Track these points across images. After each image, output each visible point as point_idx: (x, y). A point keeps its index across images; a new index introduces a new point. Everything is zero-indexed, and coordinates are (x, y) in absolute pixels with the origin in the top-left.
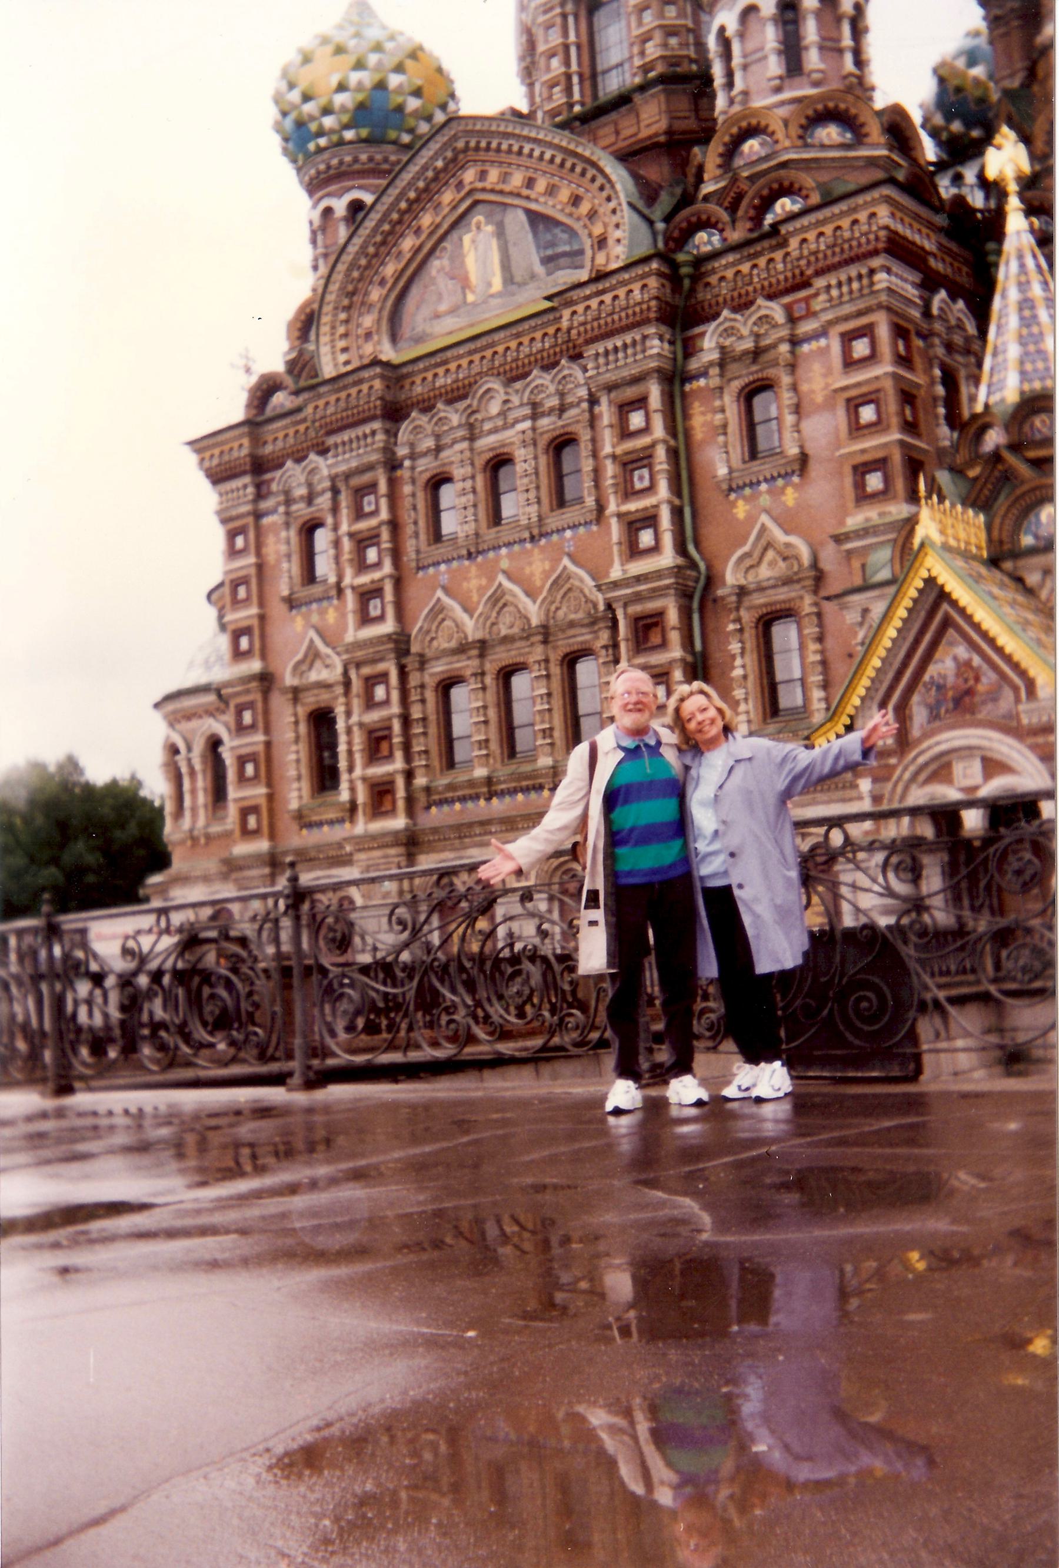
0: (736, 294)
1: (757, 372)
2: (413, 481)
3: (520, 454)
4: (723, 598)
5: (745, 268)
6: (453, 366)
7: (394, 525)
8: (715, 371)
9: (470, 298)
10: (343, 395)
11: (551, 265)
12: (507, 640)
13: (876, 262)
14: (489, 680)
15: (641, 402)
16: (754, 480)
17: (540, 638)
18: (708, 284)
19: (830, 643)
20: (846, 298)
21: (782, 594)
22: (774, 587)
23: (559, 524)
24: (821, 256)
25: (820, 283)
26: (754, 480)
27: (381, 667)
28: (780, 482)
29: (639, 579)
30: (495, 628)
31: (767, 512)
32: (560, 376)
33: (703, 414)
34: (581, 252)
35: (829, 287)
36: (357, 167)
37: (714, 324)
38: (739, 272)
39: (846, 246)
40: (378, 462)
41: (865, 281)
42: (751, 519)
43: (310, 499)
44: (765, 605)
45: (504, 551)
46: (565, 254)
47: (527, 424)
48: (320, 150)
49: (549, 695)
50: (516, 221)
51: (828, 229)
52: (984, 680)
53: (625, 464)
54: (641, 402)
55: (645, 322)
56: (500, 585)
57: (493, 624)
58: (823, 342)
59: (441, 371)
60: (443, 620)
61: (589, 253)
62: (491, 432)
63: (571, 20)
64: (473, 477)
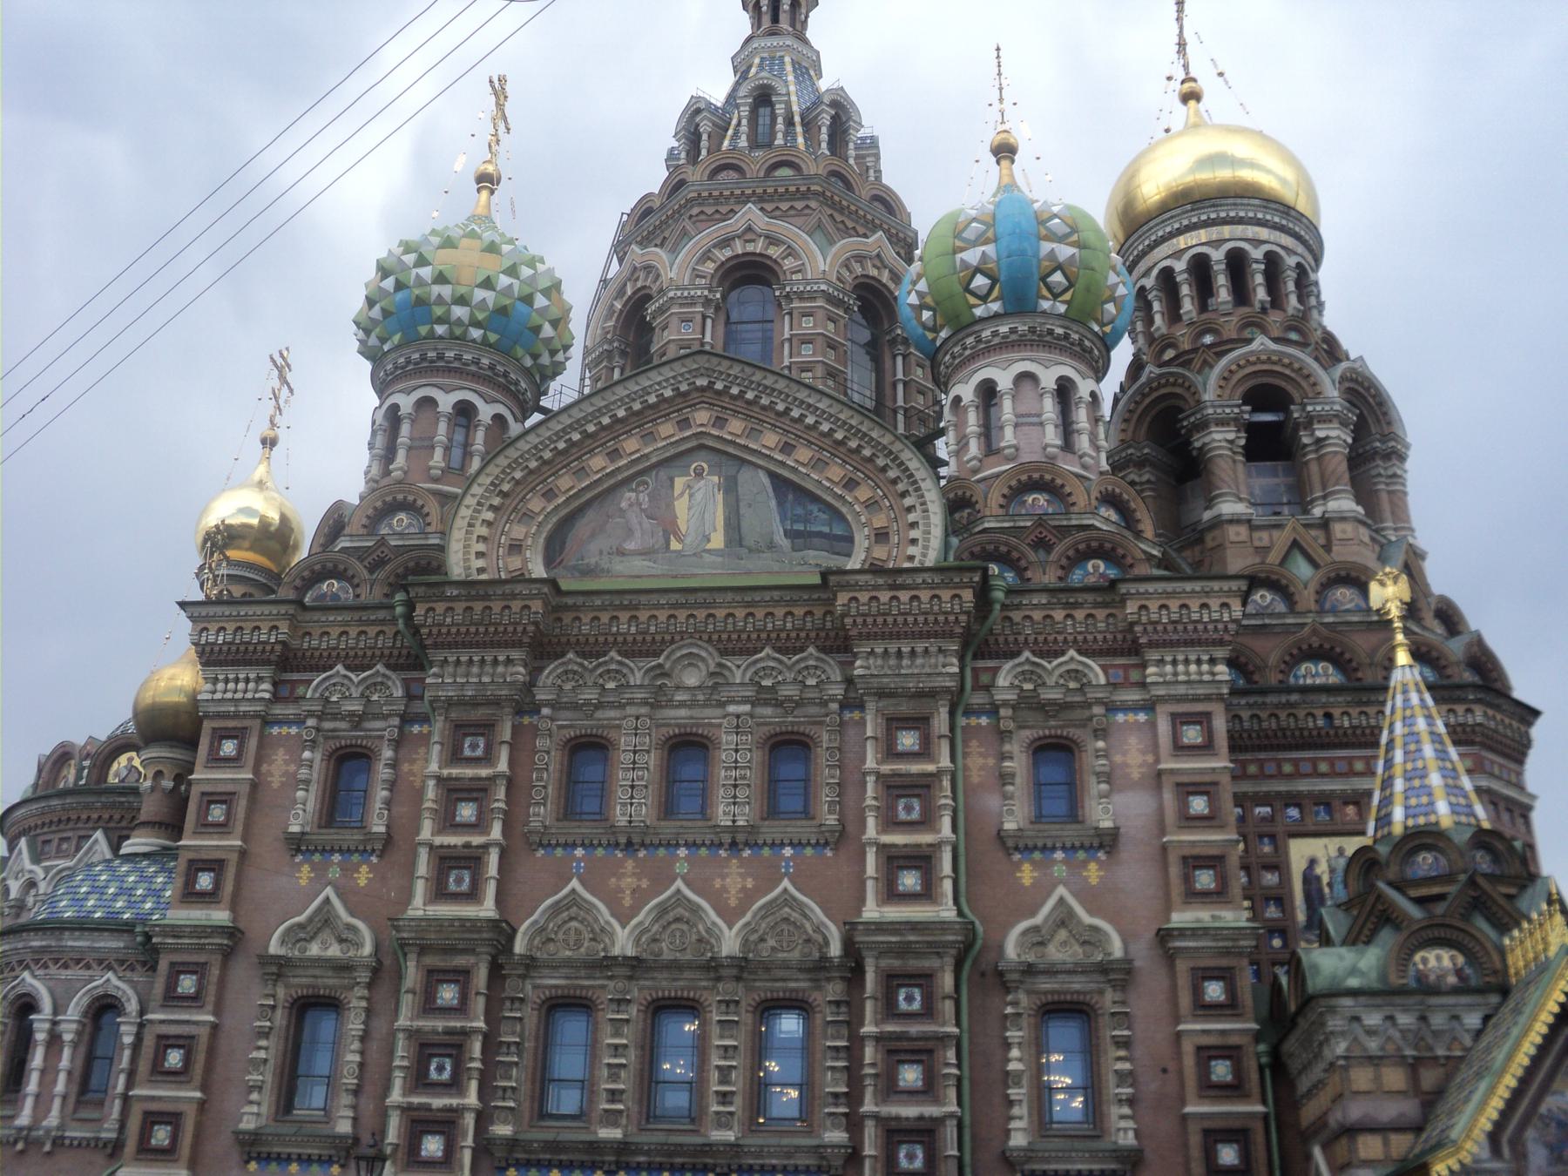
0: (1041, 638)
1: (1056, 727)
2: (550, 736)
3: (727, 739)
4: (1001, 974)
5: (1059, 615)
6: (643, 616)
7: (511, 783)
9: (675, 545)
10: (478, 606)
11: (801, 541)
12: (675, 966)
13: (1220, 653)
14: (633, 1011)
15: (920, 723)
16: (1049, 844)
17: (734, 972)
18: (1010, 619)
19: (1139, 1051)
21: (1077, 984)
22: (1069, 972)
23: (778, 838)
24: (1160, 628)
25: (1153, 655)
26: (1049, 844)
27: (460, 961)
28: (1081, 855)
29: (914, 926)
30: (655, 947)
31: (1065, 885)
32: (803, 665)
34: (850, 539)
35: (1161, 662)
36: (473, 368)
37: (1010, 664)
39: (1190, 627)
40: (509, 699)
41: (1205, 667)
42: (1043, 890)
43: (357, 720)
44: (1053, 992)
45: (682, 852)
46: (820, 534)
47: (747, 708)
48: (431, 335)
49: (735, 1047)
50: (755, 484)
51: (1174, 605)
53: (889, 787)
54: (920, 723)
55: (948, 635)
56: (678, 891)
57: (655, 940)
58: (1142, 717)
59: (624, 616)
60: (571, 919)
61: (861, 541)
62: (682, 705)
63: (709, 322)
64: (648, 752)
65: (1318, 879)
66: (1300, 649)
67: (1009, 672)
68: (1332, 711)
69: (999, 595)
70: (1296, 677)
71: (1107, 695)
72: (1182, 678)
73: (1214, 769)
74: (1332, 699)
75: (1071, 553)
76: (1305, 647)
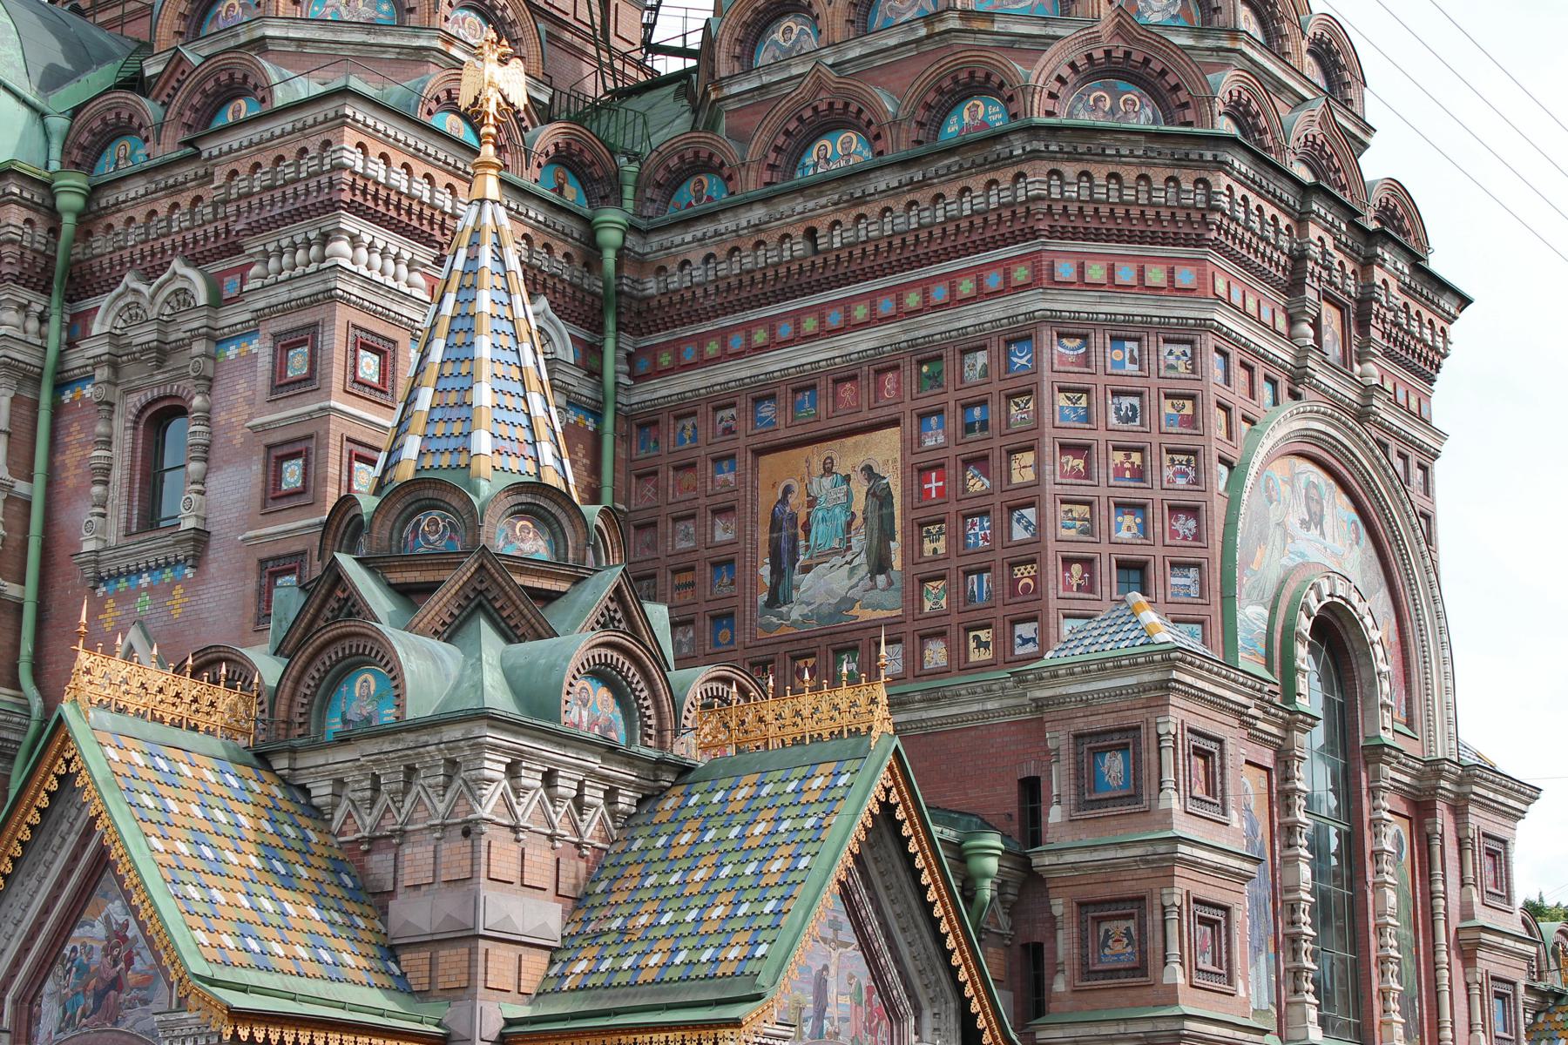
0: (147, 248)
1: (165, 383)
8: (102, 374)
18: (110, 226)
20: (285, 275)
24: (255, 201)
25: (254, 246)
28: (168, 575)
31: (142, 625)
33: (83, 446)
35: (267, 255)
37: (110, 297)
38: (153, 213)
39: (289, 191)
41: (314, 250)
51: (266, 160)
52: (138, 964)
58: (255, 346)
65: (793, 518)
66: (800, 119)
67: (107, 311)
68: (814, 224)
69: (69, 202)
70: (804, 166)
71: (204, 322)
72: (285, 275)
73: (309, 413)
74: (811, 205)
75: (197, 99)
76: (807, 114)
